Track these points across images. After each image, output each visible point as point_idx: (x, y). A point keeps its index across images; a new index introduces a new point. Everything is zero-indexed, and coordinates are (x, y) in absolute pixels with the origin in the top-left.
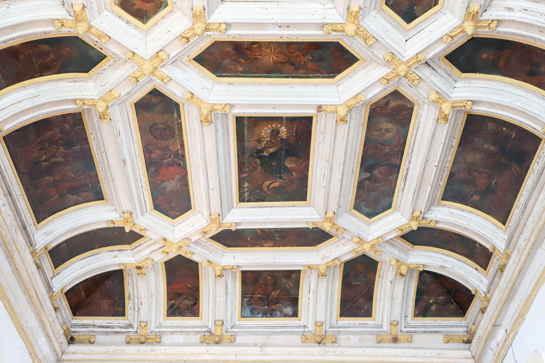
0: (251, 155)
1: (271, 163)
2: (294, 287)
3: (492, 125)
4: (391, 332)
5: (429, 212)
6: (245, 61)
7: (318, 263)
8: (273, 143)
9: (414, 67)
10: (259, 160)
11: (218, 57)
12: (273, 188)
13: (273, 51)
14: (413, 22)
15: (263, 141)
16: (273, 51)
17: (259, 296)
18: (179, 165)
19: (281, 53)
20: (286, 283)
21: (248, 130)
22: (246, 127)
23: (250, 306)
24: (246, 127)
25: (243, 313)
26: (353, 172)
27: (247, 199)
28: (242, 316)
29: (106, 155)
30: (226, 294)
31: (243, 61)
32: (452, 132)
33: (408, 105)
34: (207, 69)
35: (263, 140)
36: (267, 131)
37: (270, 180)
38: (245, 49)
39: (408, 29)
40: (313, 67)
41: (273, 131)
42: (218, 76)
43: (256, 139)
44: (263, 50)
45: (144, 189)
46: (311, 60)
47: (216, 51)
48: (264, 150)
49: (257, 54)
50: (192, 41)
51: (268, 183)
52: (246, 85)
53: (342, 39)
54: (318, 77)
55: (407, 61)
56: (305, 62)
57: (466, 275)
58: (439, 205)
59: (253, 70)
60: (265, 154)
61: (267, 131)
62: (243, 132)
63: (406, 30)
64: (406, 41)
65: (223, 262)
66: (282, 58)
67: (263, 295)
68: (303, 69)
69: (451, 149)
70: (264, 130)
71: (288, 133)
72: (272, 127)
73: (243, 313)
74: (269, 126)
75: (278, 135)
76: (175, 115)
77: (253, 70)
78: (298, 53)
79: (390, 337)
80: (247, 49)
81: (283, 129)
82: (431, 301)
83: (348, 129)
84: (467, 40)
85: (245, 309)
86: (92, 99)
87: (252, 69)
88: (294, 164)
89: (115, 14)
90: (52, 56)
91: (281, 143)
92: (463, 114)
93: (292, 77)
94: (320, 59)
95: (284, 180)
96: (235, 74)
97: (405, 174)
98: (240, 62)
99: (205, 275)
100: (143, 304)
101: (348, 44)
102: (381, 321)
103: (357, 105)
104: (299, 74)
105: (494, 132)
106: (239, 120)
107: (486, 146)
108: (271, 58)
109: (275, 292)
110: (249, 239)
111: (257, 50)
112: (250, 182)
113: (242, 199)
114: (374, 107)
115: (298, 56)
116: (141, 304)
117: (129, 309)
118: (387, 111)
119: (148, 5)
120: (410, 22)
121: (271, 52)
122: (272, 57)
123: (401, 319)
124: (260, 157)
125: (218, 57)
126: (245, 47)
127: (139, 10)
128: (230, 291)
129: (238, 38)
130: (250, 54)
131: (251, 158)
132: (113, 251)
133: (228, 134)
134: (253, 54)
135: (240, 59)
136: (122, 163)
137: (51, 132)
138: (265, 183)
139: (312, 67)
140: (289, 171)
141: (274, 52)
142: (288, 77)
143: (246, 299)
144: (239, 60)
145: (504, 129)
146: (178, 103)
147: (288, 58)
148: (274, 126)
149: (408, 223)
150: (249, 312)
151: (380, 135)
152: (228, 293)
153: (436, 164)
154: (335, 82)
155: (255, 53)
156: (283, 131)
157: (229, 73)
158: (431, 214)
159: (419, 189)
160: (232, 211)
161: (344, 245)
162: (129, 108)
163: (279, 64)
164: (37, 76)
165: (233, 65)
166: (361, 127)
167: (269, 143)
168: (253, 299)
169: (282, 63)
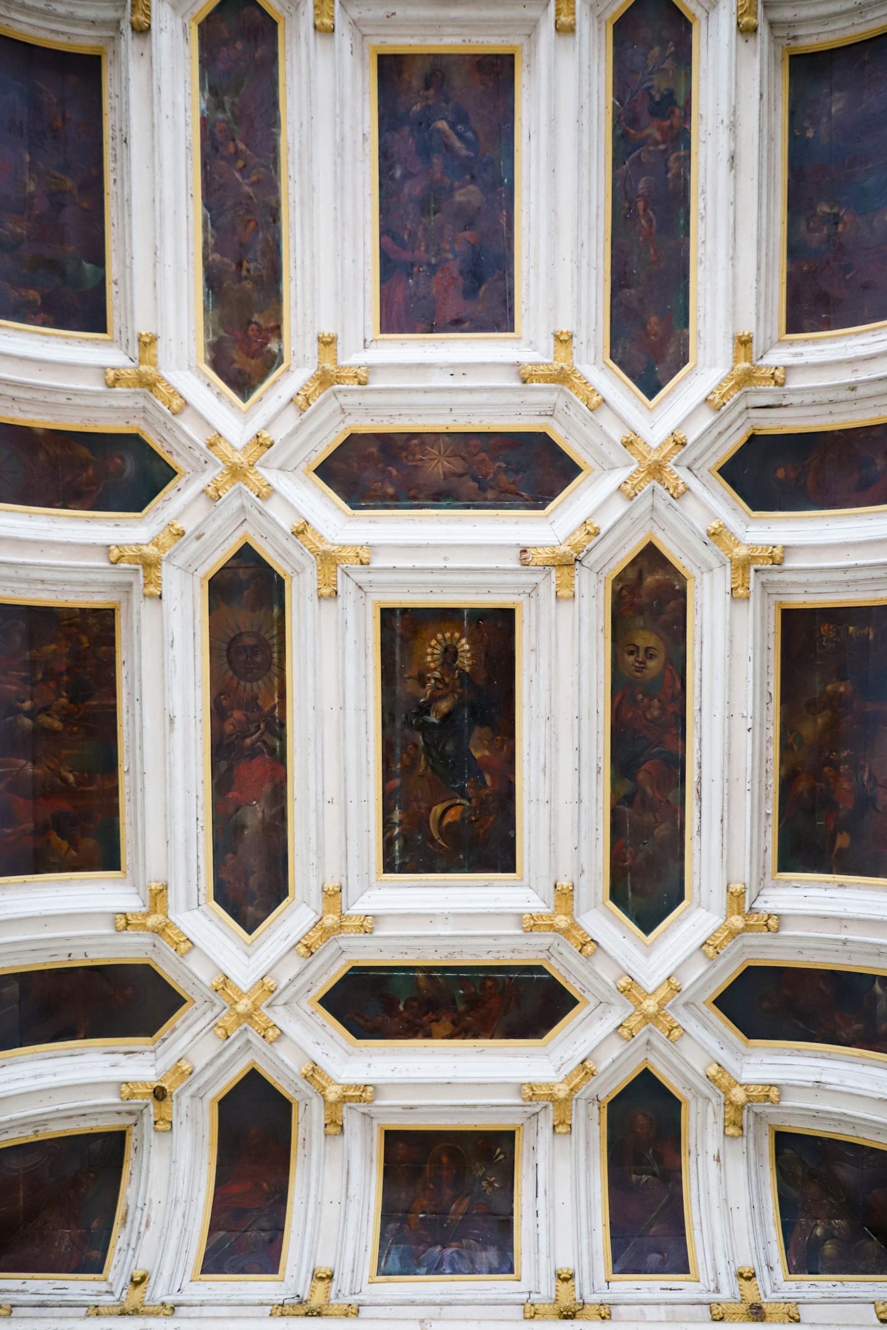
0: (407, 723)
1: (444, 747)
2: (500, 1188)
3: (829, 630)
4: (742, 1295)
5: (759, 899)
6: (398, 471)
7: (549, 1080)
8: (446, 685)
10: (421, 738)
12: (449, 824)
13: (442, 451)
15: (429, 679)
16: (442, 451)
17: (421, 1216)
18: (272, 751)
19: (455, 456)
20: (483, 1178)
21: (402, 649)
23: (402, 1246)
24: (398, 641)
25: (383, 1264)
26: (598, 772)
27: (398, 862)
28: (381, 1272)
29: (141, 704)
30: (347, 1197)
31: (394, 472)
32: (762, 626)
33: (676, 583)
34: (337, 492)
35: (429, 675)
36: (435, 651)
37: (443, 802)
41: (446, 650)
42: (353, 508)
43: (416, 674)
44: (426, 449)
45: (200, 824)
46: (506, 470)
48: (430, 706)
50: (313, 405)
51: (438, 809)
54: (518, 508)
56: (494, 474)
57: (875, 1088)
58: (777, 884)
59: (412, 493)
60: (433, 719)
61: (435, 651)
62: (392, 654)
65: (345, 1075)
66: (457, 466)
67: (432, 1213)
68: (492, 487)
69: (769, 705)
70: (430, 646)
71: (472, 657)
72: (444, 639)
73: (383, 1264)
74: (439, 636)
75: (455, 662)
76: (276, 610)
78: (483, 455)
79: (744, 1308)
81: (464, 645)
82: (819, 1231)
84: (746, 439)
85: (389, 1253)
86: (137, 544)
87: (410, 490)
88: (488, 749)
90: (91, 472)
91: (461, 687)
92: (773, 608)
95: (470, 800)
97: (696, 779)
98: (391, 473)
99: (304, 1148)
100: (152, 1224)
102: (713, 1280)
103: (589, 546)
104: (486, 499)
105: (834, 644)
106: (387, 615)
107: (829, 688)
108: (440, 465)
109: (459, 1204)
110: (401, 1008)
111: (418, 449)
112: (403, 809)
113: (389, 867)
114: (620, 586)
115: (484, 460)
116: (147, 1225)
117: (117, 1251)
119: (253, 362)
123: (760, 1266)
124: (425, 728)
125: (355, 464)
127: (240, 372)
128: (354, 1189)
130: (406, 457)
131: (407, 731)
132: (114, 1053)
133: (366, 656)
134: (410, 457)
135: (390, 468)
136: (167, 720)
137: (53, 647)
138: (434, 808)
140: (477, 769)
143: (391, 1226)
145: (851, 629)
146: (281, 574)
147: (467, 465)
148: (448, 635)
149: (723, 924)
150: (397, 1262)
151: (637, 664)
152: (351, 1193)
153: (749, 787)
155: (414, 455)
156: (463, 651)
158: (766, 902)
159: (729, 803)
160: (368, 893)
161: (601, 1019)
162: (198, 590)
164: (58, 505)
166: (601, 636)
167: (440, 686)
168: (409, 1225)
169: (461, 475)
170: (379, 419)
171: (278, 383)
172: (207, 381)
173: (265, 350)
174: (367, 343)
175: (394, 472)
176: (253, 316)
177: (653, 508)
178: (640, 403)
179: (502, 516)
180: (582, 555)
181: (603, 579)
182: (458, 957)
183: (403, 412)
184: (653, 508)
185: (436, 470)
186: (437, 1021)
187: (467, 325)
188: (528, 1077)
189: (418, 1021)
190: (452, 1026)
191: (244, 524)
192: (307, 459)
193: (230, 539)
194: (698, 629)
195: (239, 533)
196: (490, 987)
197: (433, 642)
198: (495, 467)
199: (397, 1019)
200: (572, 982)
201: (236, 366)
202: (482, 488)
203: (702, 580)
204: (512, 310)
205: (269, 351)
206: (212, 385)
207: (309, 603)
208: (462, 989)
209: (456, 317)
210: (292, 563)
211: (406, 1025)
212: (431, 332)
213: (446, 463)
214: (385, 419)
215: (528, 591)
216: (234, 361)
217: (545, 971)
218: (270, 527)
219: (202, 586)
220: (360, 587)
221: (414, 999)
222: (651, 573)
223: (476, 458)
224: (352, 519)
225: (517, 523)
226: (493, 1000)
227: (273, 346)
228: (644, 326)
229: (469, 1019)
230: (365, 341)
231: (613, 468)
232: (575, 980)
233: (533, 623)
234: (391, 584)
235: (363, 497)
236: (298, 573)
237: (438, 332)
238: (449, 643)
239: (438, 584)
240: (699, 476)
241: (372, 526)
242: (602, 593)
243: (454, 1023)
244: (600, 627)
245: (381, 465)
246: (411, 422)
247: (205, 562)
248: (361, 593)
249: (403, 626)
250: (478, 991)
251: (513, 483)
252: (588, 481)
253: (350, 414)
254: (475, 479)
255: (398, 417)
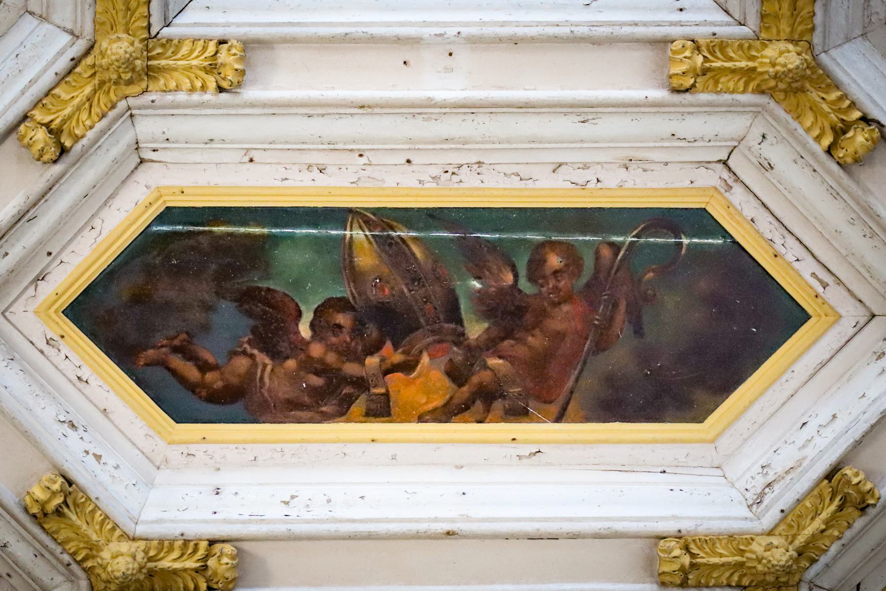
110: (304, 330)
182: (470, 179)
186: (407, 367)
188: (674, 517)
189: (351, 369)
190: (447, 382)
196: (556, 273)
199: (291, 364)
200: (790, 258)
208: (478, 278)
211: (317, 381)
217: (713, 227)
221: (341, 304)
226: (566, 308)
229: (494, 362)
232: (801, 252)
243: (457, 375)
250: (524, 285)
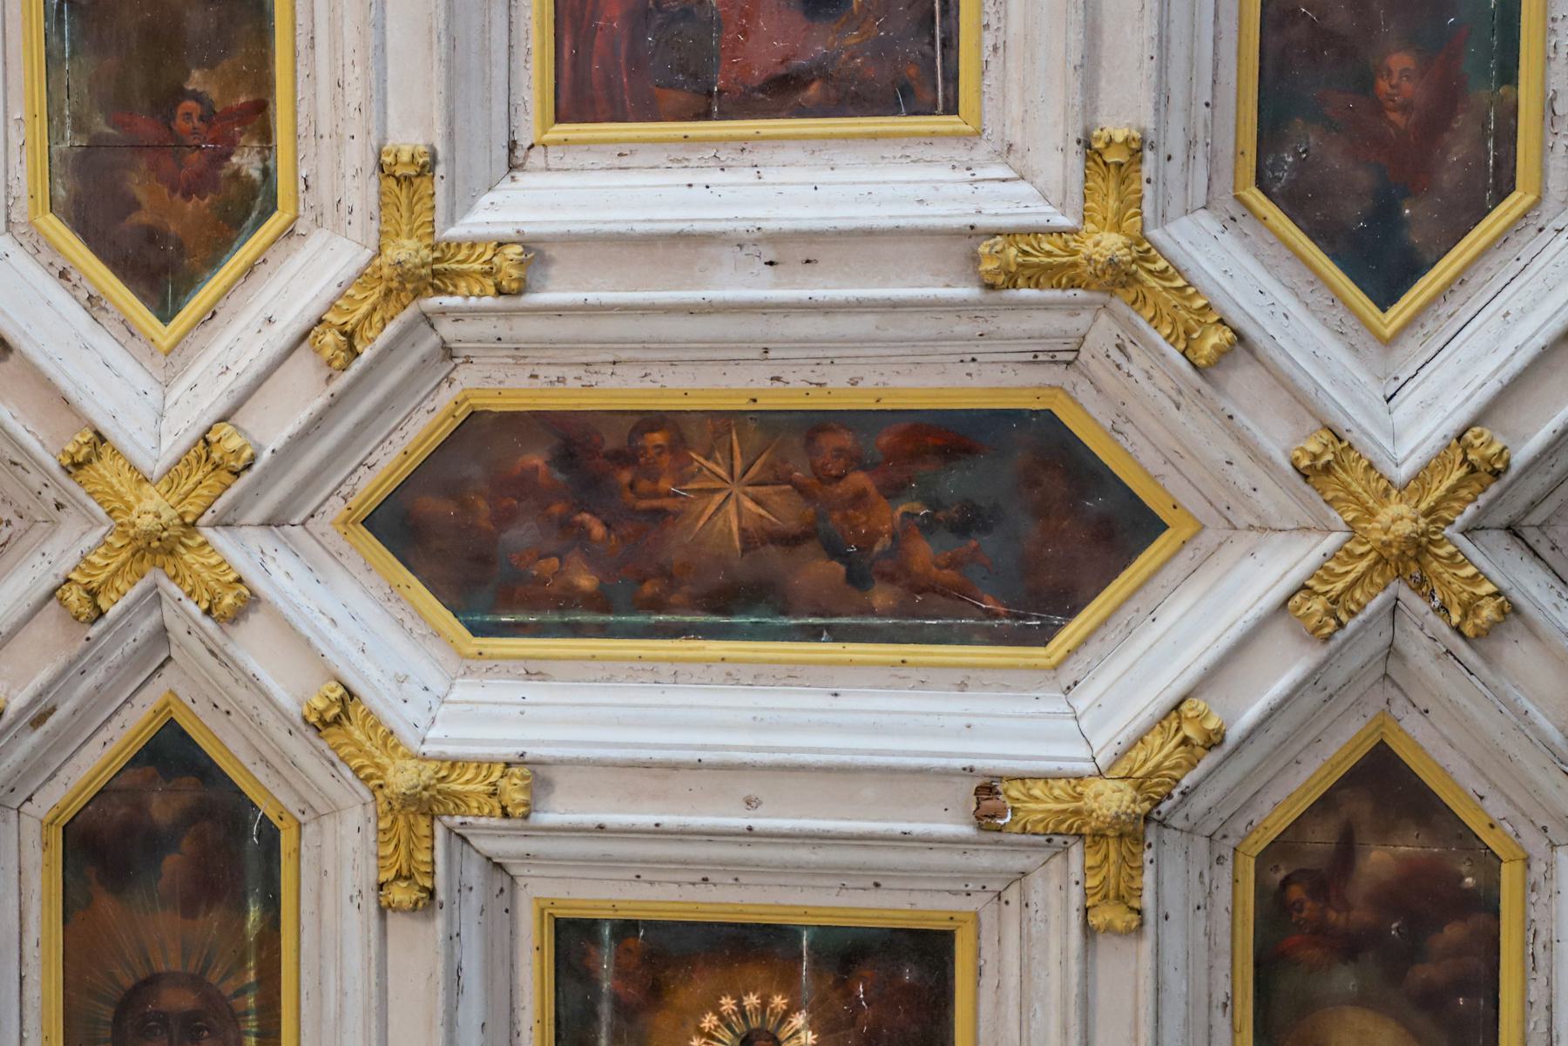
6: (608, 525)
9: (1459, 520)
11: (482, 505)
13: (738, 469)
14: (1405, 300)
16: (738, 469)
19: (777, 481)
22: (605, 1009)
31: (598, 530)
38: (606, 456)
39: (1388, 332)
40: (940, 568)
42: (477, 630)
44: (692, 459)
46: (928, 527)
47: (475, 471)
49: (665, 484)
52: (608, 680)
53: (1068, 387)
54: (964, 638)
55: (1416, 477)
56: (893, 538)
59: (649, 589)
63: (1379, 337)
64: (1388, 401)
66: (784, 511)
68: (890, 578)
74: (728, 1004)
77: (649, 589)
78: (859, 479)
80: (626, 457)
83: (1150, 1018)
87: (643, 581)
89: (45, 257)
93: (841, 635)
94: (969, 521)
96: (556, 618)
98: (584, 533)
101: (1099, 418)
103: (1185, 782)
104: (871, 612)
108: (731, 507)
111: (666, 460)
114: (1280, 875)
115: (860, 497)
118: (1354, 914)
119: (190, 206)
120: (1393, 300)
121: (731, 475)
122: (737, 500)
125: (482, 505)
126: (611, 443)
127: (152, 236)
129: (578, 384)
130: (632, 486)
134: (644, 485)
135: (586, 517)
139: (934, 569)
141: (745, 473)
142: (813, 634)
144: (582, 525)
148: (752, 1000)
154: (1054, 660)
157: (533, 605)
163: (772, 549)
165: (547, 556)
166: (1222, 1023)
169: (790, 541)
170: (554, 373)
171: (262, 270)
172: (60, 264)
173: (225, 172)
174: (519, 153)
175: (598, 530)
176: (187, 74)
177: (1391, 650)
178: (1350, 321)
179: (918, 665)
180: (1165, 806)
181: (1228, 853)
183: (624, 356)
184: (1391, 650)
185: (720, 523)
187: (814, 90)
191: (166, 671)
192: (345, 490)
193: (126, 712)
194: (1538, 1017)
195: (152, 696)
197: (709, 1021)
198: (897, 514)
201: (143, 217)
202: (858, 578)
203: (1550, 865)
204: (950, 43)
205: (236, 175)
206: (74, 276)
207: (351, 911)
209: (781, 71)
210: (301, 787)
212: (706, 115)
213: (749, 504)
214: (570, 373)
215: (998, 886)
216: (135, 205)
218: (241, 692)
219: (46, 845)
220: (499, 866)
222: (1384, 834)
223: (839, 489)
224: (474, 664)
225: (963, 686)
227: (246, 162)
228: (1365, 83)
230: (512, 146)
231: (1265, 528)
233: (1012, 981)
234: (588, 862)
235: (507, 599)
236: (318, 816)
237: (724, 116)
238: (755, 1022)
239: (724, 865)
240: (1543, 549)
241: (535, 692)
242: (1224, 896)
244: (1220, 997)
245: (556, 509)
246: (647, 384)
247: (54, 775)
248: (501, 881)
249: (621, 973)
251: (954, 563)
252: (1182, 562)
253: (468, 360)
254: (834, 550)
255: (609, 369)
